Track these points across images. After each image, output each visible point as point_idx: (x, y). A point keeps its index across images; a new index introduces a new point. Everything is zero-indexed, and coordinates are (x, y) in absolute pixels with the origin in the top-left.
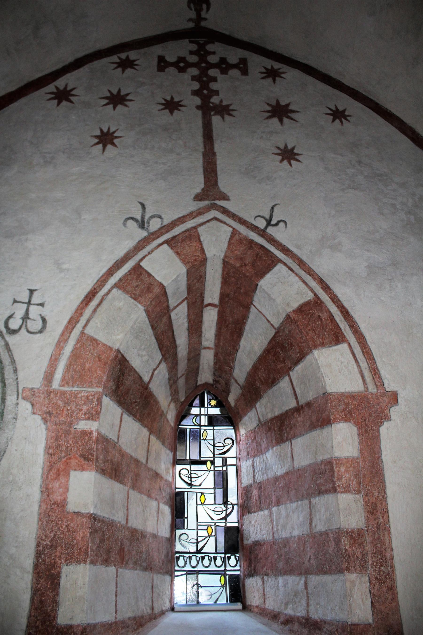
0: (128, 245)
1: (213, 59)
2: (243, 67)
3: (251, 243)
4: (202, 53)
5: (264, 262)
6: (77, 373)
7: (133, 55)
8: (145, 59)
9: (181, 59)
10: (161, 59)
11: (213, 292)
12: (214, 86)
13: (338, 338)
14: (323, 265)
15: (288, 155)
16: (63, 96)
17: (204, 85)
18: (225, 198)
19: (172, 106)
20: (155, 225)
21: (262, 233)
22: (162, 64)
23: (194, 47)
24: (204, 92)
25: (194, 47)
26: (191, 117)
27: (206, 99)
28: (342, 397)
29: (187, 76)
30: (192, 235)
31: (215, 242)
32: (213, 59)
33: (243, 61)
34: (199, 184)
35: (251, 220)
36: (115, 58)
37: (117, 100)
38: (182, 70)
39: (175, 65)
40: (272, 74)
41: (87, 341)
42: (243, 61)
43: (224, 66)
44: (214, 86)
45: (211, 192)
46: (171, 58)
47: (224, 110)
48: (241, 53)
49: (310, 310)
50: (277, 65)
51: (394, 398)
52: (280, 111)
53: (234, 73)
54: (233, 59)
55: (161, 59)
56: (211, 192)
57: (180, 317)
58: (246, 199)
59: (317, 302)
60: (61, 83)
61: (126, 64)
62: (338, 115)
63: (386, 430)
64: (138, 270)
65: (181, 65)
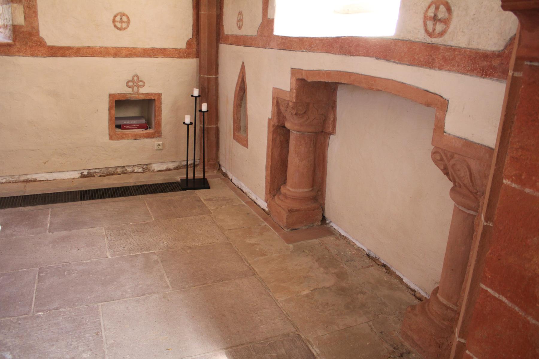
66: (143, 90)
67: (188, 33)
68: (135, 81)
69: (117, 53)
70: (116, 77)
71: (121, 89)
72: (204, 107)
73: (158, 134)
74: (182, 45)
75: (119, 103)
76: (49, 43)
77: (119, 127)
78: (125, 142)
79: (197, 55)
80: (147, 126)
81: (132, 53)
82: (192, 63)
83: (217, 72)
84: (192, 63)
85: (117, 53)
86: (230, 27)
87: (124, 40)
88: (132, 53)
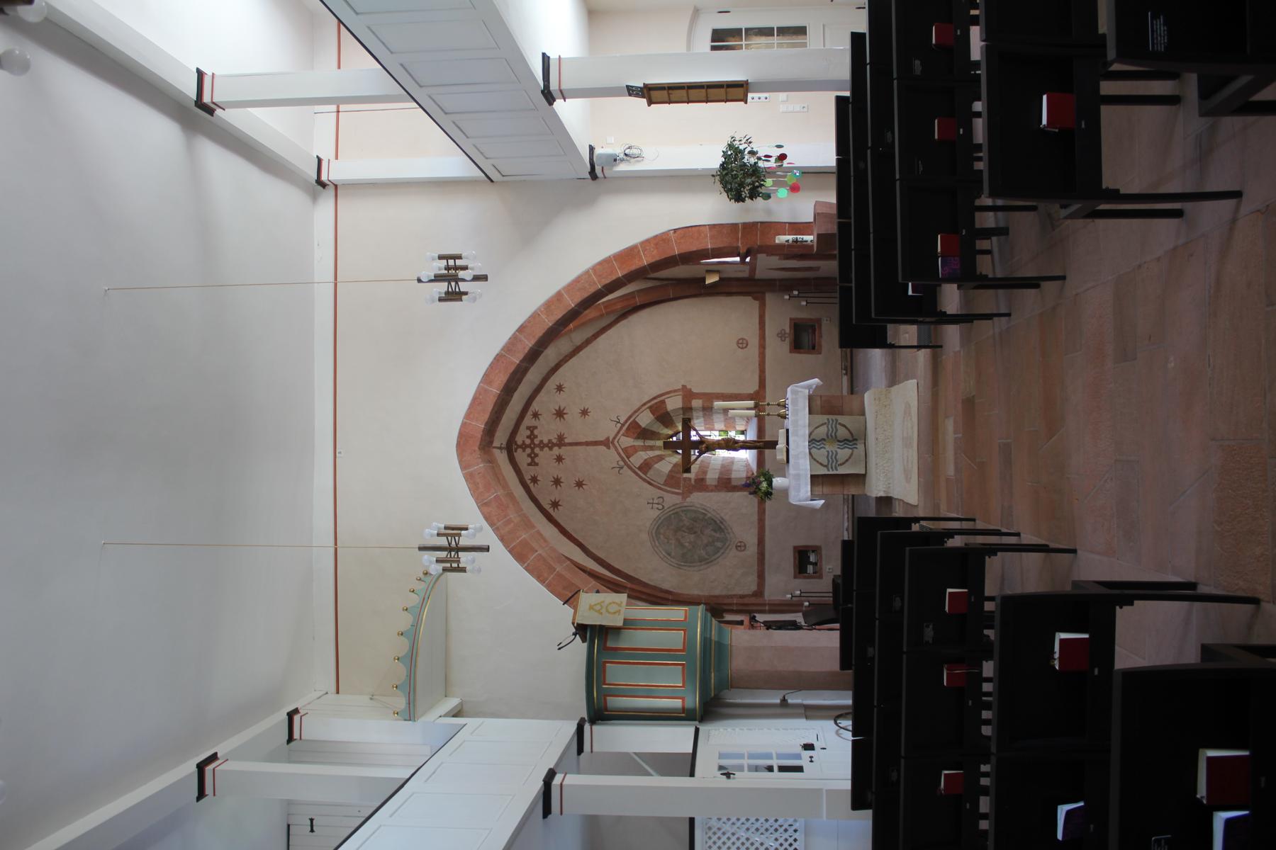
0: (630, 472)
1: (528, 441)
2: (532, 429)
3: (628, 429)
4: (524, 446)
5: (635, 425)
6: (677, 485)
7: (527, 478)
8: (528, 473)
9: (529, 455)
10: (529, 465)
11: (639, 443)
12: (546, 441)
13: (663, 402)
14: (638, 405)
15: (585, 412)
16: (555, 504)
17: (547, 445)
18: (608, 439)
19: (559, 459)
20: (622, 463)
21: (623, 425)
22: (533, 463)
23: (520, 450)
24: (550, 445)
25: (520, 450)
26: (563, 451)
27: (555, 445)
28: (684, 403)
29: (541, 453)
30: (625, 450)
31: (628, 442)
32: (528, 441)
33: (528, 428)
34: (603, 448)
35: (616, 430)
36: (531, 485)
37: (557, 482)
38: (536, 455)
39: (533, 459)
40: (536, 415)
41: (666, 483)
42: (528, 428)
43: (532, 436)
44: (546, 441)
45: (606, 443)
46: (529, 460)
47: (561, 438)
48: (523, 427)
49: (653, 410)
50: (530, 413)
51: (684, 386)
52: (560, 414)
53: (536, 432)
54: (528, 433)
55: (529, 465)
56: (606, 443)
57: (651, 454)
58: (609, 430)
59: (650, 408)
60: (547, 507)
61: (534, 480)
62: (560, 388)
63: (695, 391)
64: (640, 468)
65: (533, 456)
66: (788, 331)
67: (749, 299)
68: (781, 335)
69: (762, 346)
70: (778, 349)
71: (786, 346)
72: (796, 293)
73: (819, 321)
74: (756, 304)
75: (797, 346)
76: (756, 388)
77: (814, 348)
78: (823, 343)
79: (764, 293)
80: (814, 331)
81: (762, 337)
82: (769, 298)
83: (775, 280)
84: (769, 298)
85: (762, 346)
86: (746, 275)
87: (754, 342)
88: (762, 337)
